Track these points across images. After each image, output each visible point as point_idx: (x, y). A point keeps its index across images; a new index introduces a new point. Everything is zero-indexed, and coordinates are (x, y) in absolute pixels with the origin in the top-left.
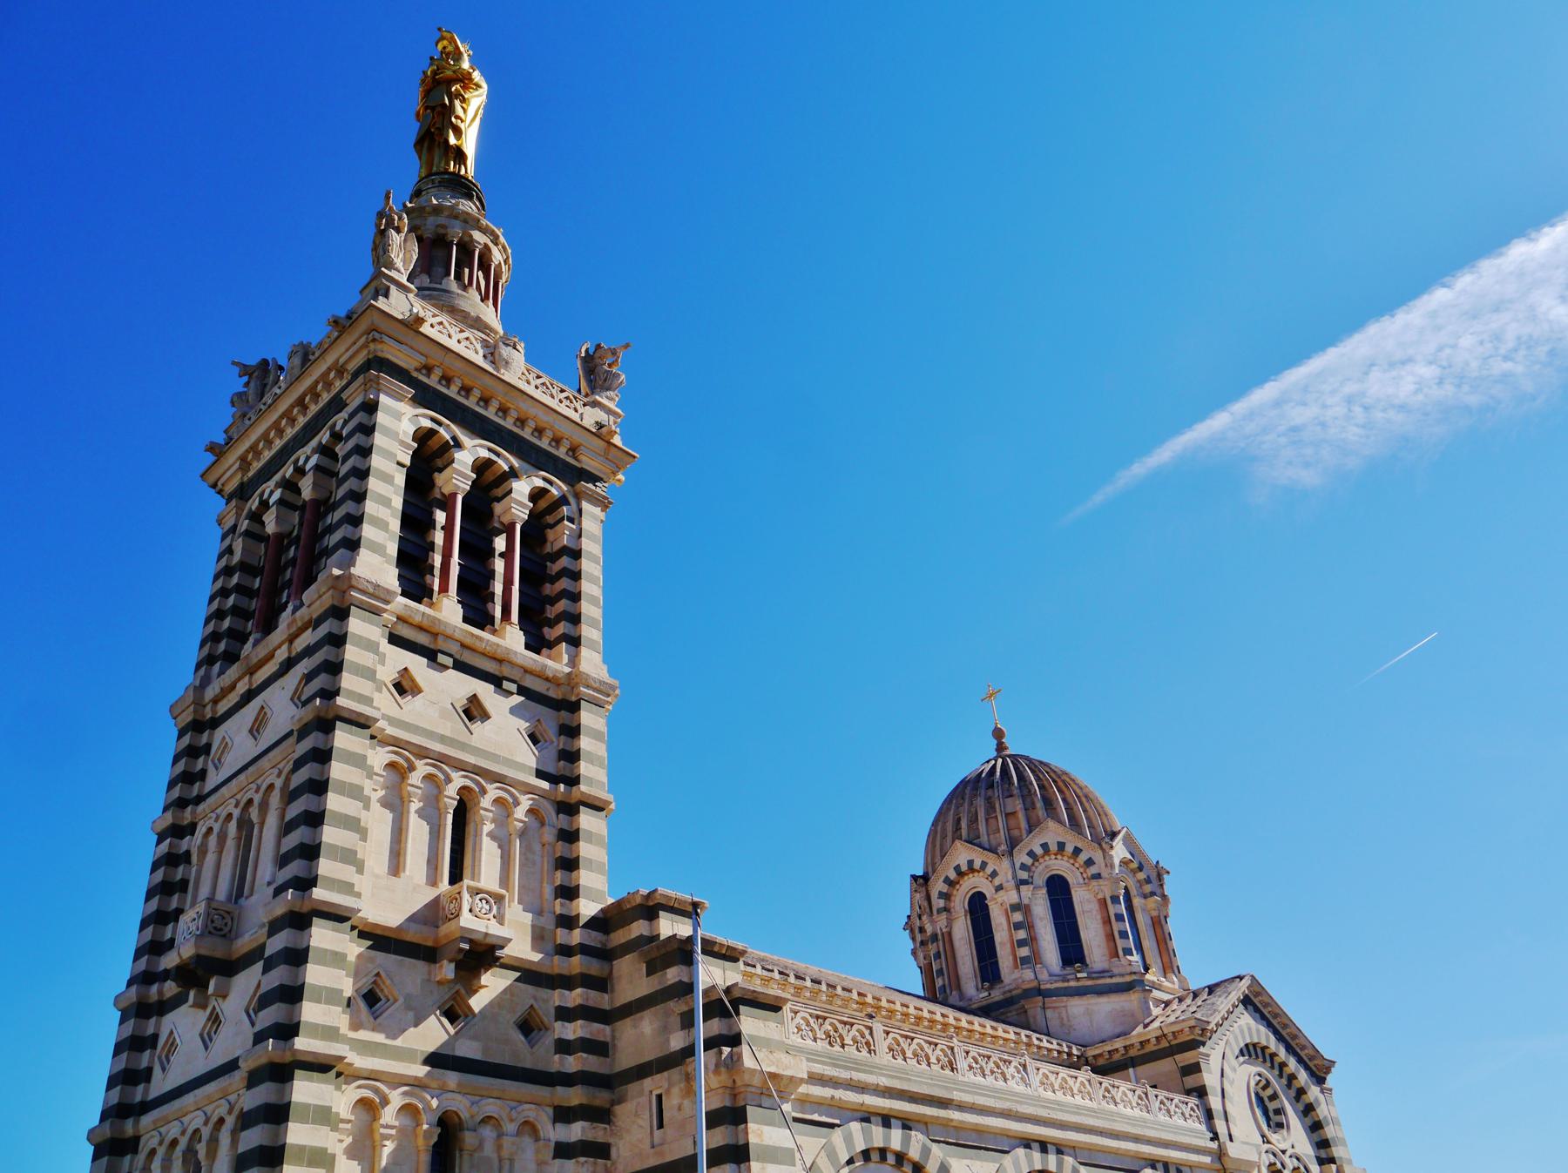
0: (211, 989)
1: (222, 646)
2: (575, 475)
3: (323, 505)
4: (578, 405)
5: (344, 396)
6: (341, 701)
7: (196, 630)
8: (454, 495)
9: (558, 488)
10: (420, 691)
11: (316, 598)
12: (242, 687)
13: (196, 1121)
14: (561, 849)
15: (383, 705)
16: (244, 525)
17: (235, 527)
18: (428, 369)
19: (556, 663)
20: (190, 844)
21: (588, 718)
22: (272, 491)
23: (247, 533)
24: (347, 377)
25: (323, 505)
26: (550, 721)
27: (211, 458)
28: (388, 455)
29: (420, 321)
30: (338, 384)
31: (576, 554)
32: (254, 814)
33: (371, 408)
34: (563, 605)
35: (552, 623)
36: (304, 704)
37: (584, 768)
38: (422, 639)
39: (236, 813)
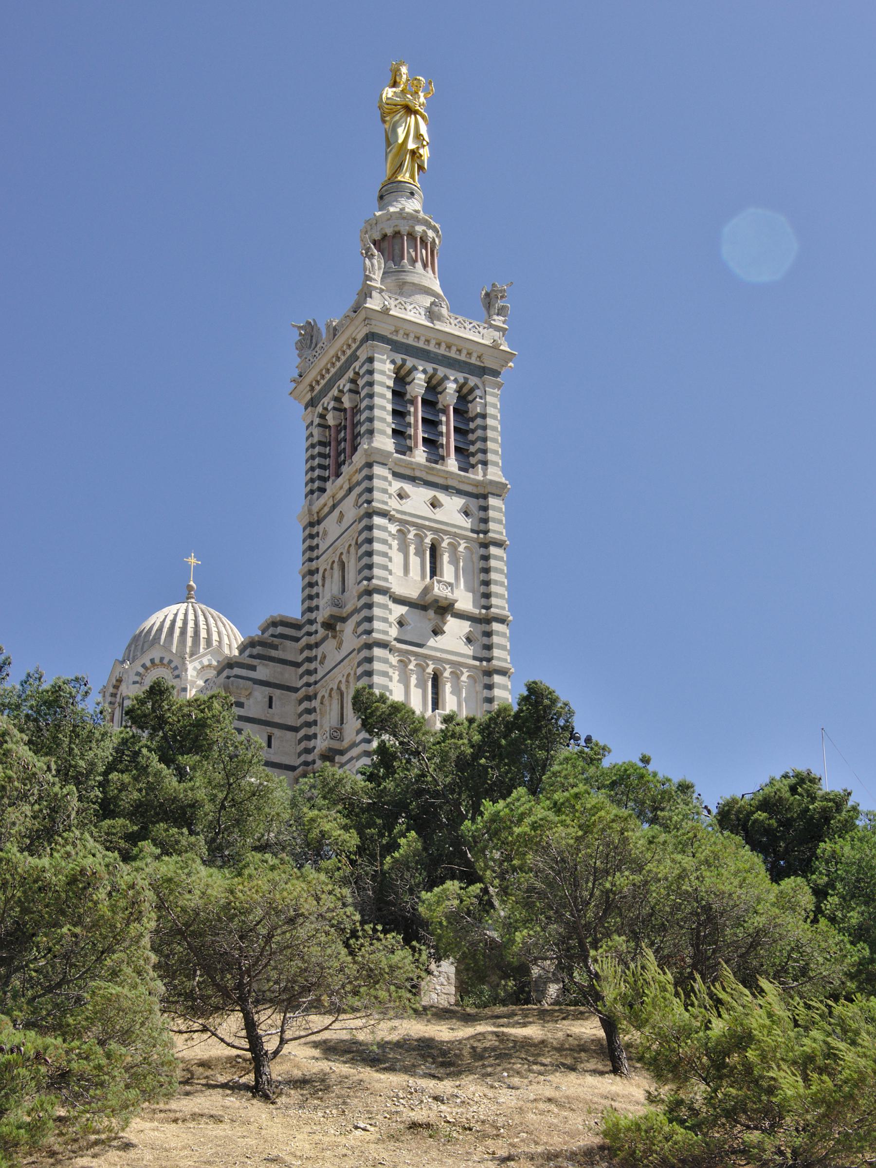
0: (338, 628)
1: (317, 484)
2: (482, 371)
3: (356, 410)
4: (481, 329)
5: (358, 353)
6: (374, 504)
7: (302, 478)
8: (416, 397)
9: (473, 381)
10: (409, 497)
11: (358, 459)
12: (330, 503)
13: (340, 678)
14: (482, 564)
15: (394, 504)
16: (317, 421)
17: (312, 422)
18: (397, 331)
19: (477, 475)
20: (318, 577)
21: (492, 501)
22: (328, 401)
23: (319, 425)
24: (358, 343)
25: (356, 410)
26: (474, 504)
27: (294, 385)
28: (382, 384)
29: (388, 310)
30: (354, 346)
31: (484, 416)
32: (344, 557)
33: (371, 360)
34: (479, 445)
35: (473, 455)
36: (359, 507)
37: (492, 526)
38: (408, 472)
39: (337, 560)
